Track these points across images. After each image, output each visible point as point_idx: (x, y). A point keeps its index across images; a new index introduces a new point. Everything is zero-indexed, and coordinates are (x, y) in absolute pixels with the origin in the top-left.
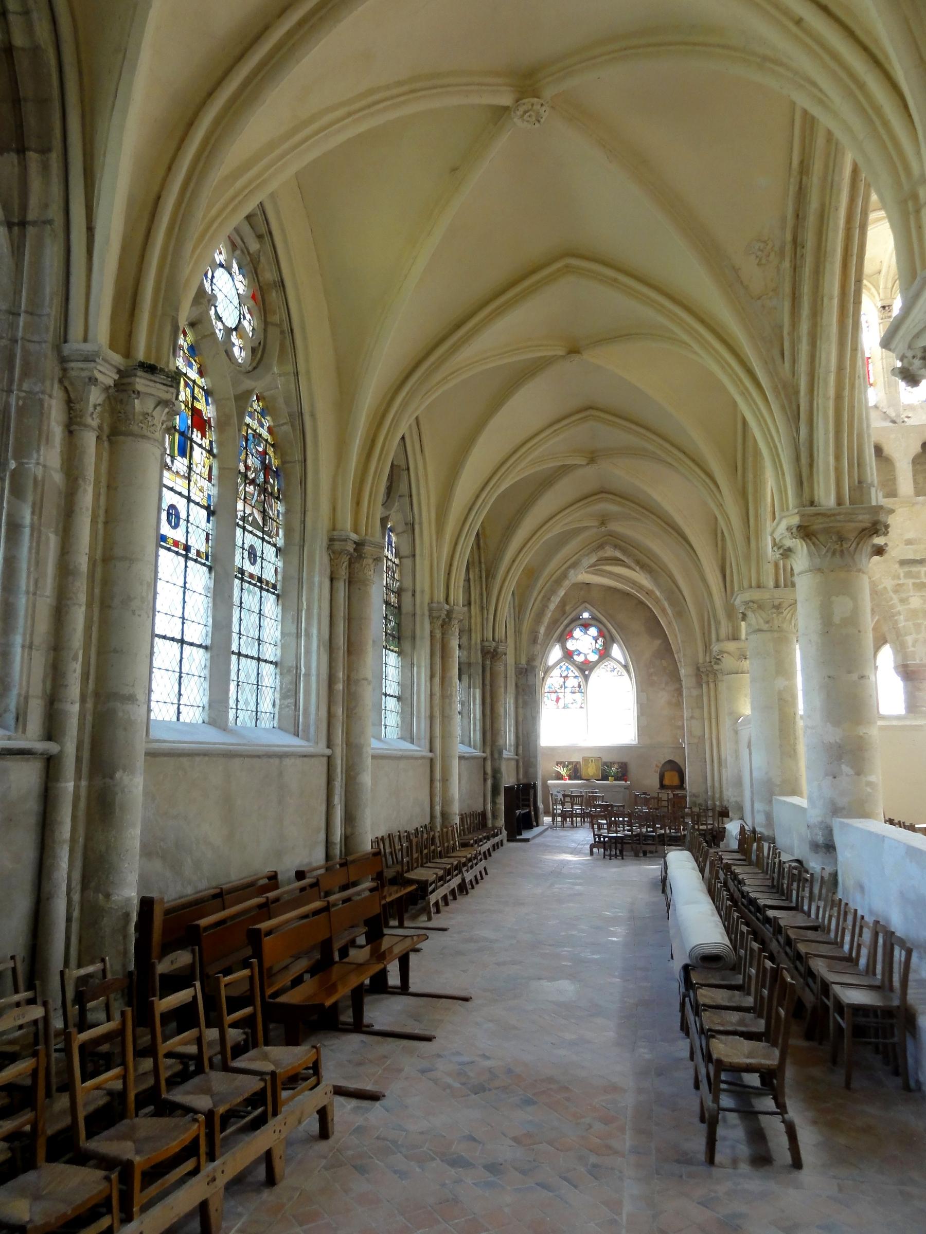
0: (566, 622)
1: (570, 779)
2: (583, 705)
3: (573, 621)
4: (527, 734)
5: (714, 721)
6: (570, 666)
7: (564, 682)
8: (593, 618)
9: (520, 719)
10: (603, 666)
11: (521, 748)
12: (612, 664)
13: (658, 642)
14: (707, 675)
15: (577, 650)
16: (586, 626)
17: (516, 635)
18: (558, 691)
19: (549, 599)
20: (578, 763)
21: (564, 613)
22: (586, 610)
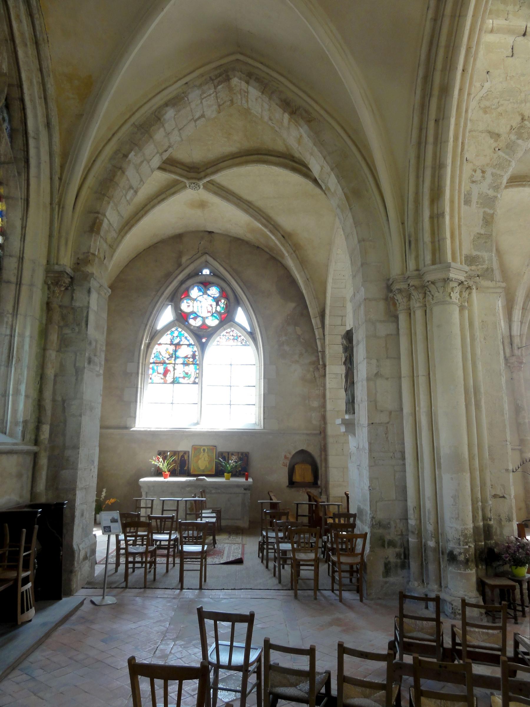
0: (181, 277)
1: (170, 476)
2: (197, 380)
3: (189, 277)
4: (64, 401)
5: (422, 381)
6: (183, 332)
7: (176, 351)
8: (215, 274)
9: (50, 372)
10: (224, 333)
11: (46, 429)
12: (235, 331)
13: (292, 305)
14: (409, 297)
15: (193, 313)
16: (205, 285)
17: (52, 210)
18: (167, 361)
19: (126, 156)
20: (185, 453)
21: (180, 265)
22: (207, 265)
